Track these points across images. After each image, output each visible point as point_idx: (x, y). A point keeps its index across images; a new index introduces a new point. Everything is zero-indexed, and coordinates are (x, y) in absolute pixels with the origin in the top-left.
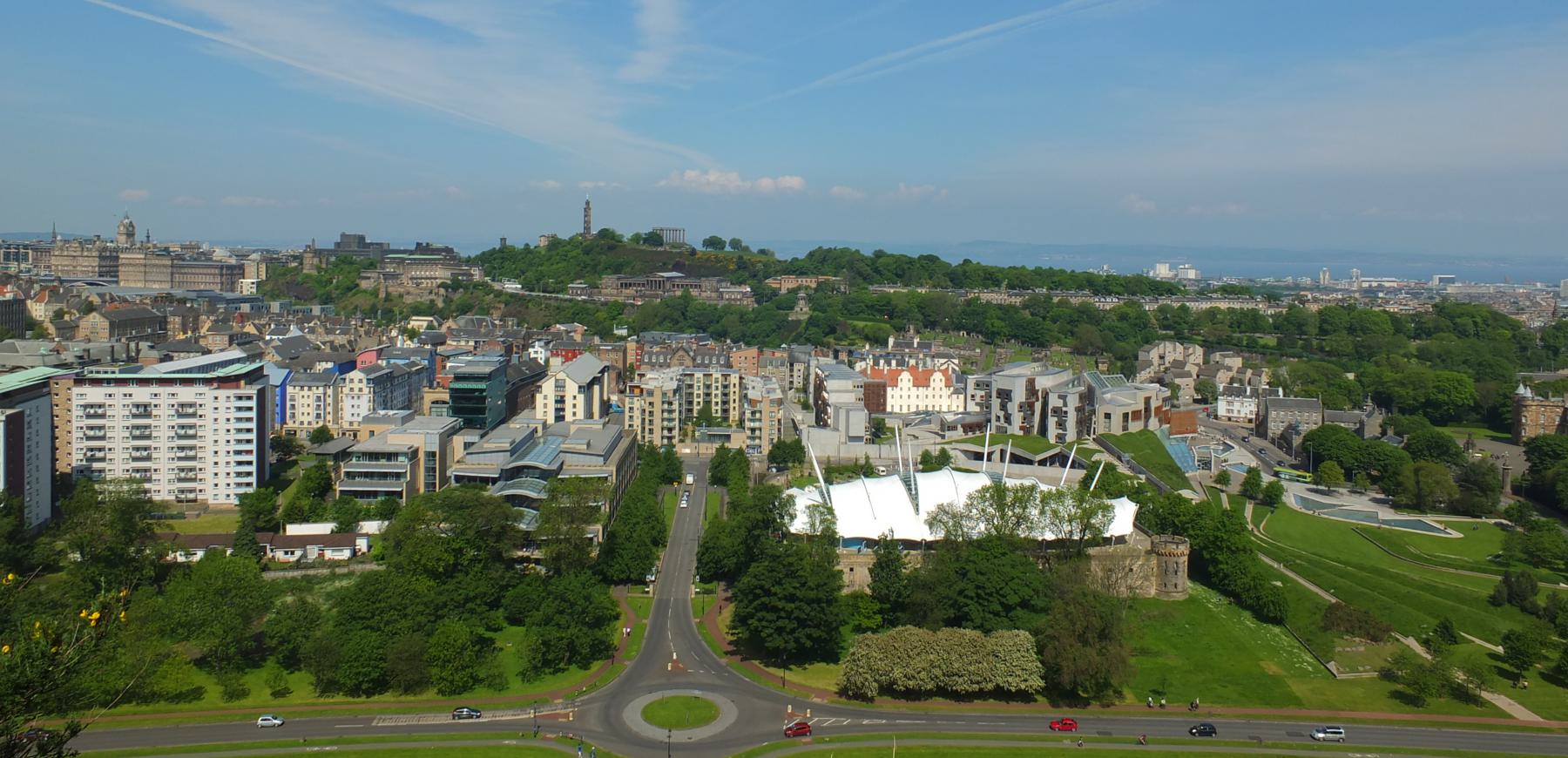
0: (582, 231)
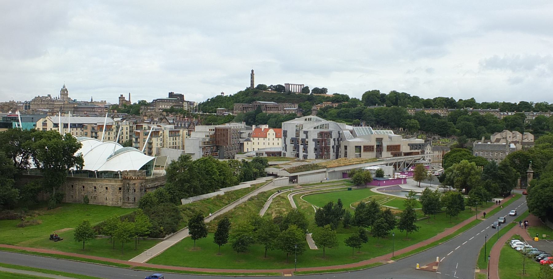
0: (249, 86)
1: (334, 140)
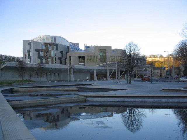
1: (61, 52)
